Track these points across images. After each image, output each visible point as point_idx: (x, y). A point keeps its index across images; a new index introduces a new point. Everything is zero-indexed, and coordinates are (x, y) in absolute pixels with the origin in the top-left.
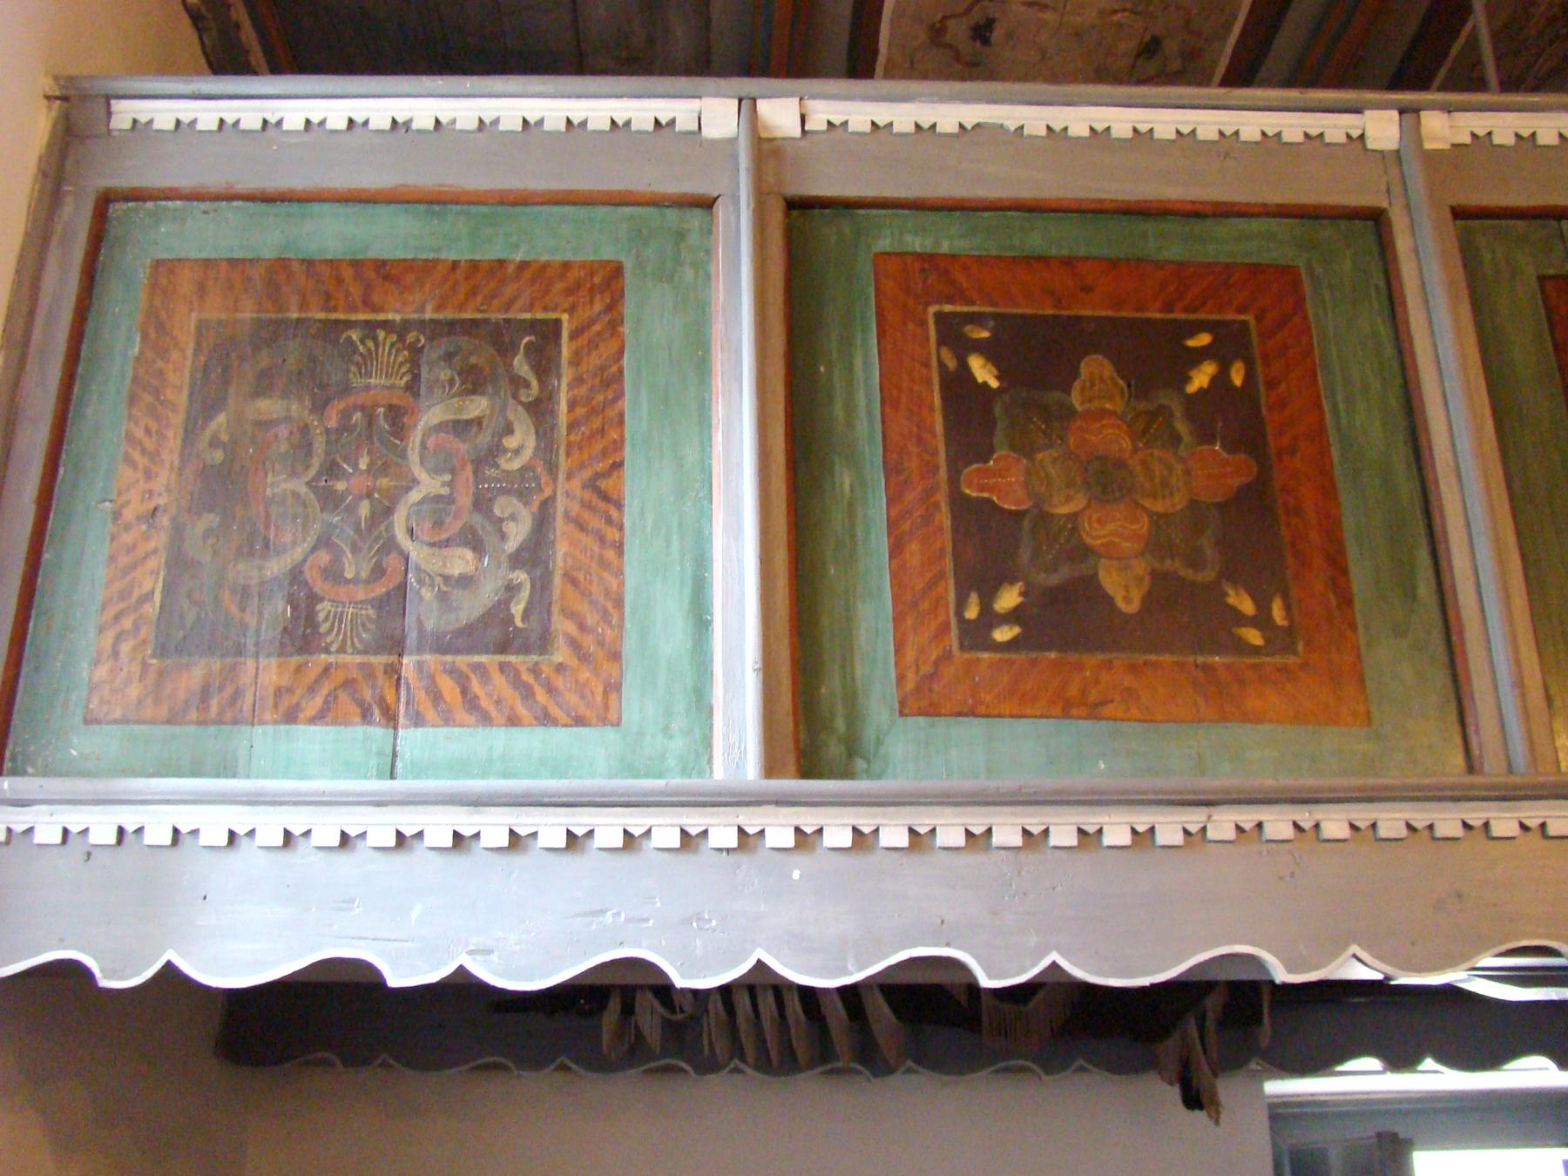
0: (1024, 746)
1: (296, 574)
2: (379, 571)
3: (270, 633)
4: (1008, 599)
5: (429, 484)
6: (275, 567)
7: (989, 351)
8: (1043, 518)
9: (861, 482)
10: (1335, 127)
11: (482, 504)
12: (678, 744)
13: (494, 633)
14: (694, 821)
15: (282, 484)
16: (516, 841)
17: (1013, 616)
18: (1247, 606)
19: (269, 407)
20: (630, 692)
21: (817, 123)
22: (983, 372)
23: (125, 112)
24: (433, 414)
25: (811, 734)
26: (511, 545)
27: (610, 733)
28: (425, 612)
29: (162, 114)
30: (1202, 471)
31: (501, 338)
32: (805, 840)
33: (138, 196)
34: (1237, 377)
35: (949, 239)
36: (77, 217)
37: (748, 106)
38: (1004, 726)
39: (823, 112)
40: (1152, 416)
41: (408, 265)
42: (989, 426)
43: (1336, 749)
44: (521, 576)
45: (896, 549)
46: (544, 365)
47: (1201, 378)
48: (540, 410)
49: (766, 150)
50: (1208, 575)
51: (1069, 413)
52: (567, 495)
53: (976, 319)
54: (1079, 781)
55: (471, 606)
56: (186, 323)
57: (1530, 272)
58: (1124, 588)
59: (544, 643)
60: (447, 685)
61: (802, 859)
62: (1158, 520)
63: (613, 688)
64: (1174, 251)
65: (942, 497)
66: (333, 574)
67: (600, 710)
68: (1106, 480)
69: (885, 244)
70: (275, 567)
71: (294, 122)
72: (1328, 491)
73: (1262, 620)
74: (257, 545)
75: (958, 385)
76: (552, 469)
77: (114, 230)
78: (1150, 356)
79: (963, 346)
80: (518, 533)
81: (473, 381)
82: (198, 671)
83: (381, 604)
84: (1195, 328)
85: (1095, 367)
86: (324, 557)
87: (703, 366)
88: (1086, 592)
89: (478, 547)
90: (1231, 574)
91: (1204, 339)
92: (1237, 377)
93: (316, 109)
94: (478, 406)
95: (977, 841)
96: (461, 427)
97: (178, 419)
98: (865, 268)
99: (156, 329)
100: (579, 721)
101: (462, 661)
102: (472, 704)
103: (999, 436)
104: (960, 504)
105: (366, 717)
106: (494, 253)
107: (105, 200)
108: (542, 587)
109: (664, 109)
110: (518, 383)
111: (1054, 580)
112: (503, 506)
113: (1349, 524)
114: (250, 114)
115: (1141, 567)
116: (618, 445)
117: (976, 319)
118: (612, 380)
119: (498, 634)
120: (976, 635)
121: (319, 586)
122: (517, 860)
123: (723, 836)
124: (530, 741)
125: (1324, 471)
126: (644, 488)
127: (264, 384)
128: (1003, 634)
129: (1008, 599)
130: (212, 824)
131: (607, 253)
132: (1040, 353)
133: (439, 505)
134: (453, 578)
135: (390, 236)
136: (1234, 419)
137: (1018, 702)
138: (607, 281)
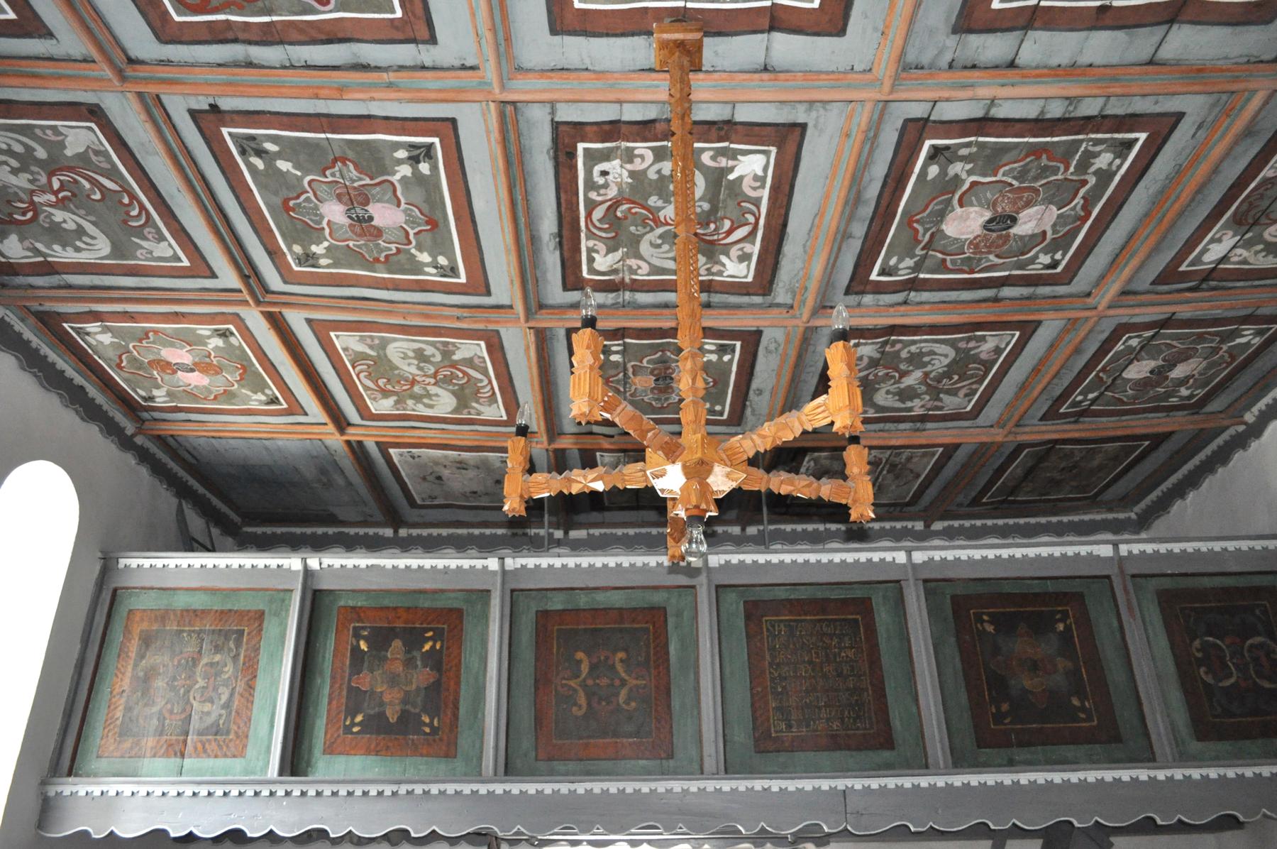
0: (357, 764)
1: (160, 712)
2: (184, 710)
3: (152, 729)
4: (359, 718)
5: (201, 683)
6: (155, 709)
7: (366, 639)
8: (373, 693)
9: (323, 682)
10: (479, 563)
11: (215, 689)
12: (261, 763)
13: (214, 730)
14: (258, 788)
16: (210, 794)
17: (359, 724)
18: (427, 720)
20: (249, 748)
21: (325, 565)
23: (123, 562)
24: (205, 661)
25: (295, 761)
26: (222, 702)
27: (242, 760)
28: (195, 724)
29: (134, 563)
32: (288, 794)
33: (127, 588)
34: (438, 647)
36: (106, 596)
37: (304, 560)
38: (351, 758)
39: (327, 561)
40: (410, 659)
41: (203, 611)
42: (363, 661)
43: (441, 766)
44: (223, 712)
45: (330, 703)
46: (238, 645)
47: (427, 647)
49: (308, 573)
50: (417, 711)
51: (386, 658)
53: (363, 628)
54: (369, 776)
55: (210, 720)
57: (534, 609)
58: (392, 715)
59: (228, 733)
60: (199, 745)
61: (287, 799)
62: (407, 693)
63: (245, 746)
64: (427, 604)
65: (345, 687)
66: (171, 712)
67: (240, 754)
68: (393, 681)
69: (342, 603)
70: (155, 709)
71: (172, 566)
72: (458, 684)
73: (431, 725)
75: (356, 650)
76: (236, 678)
77: (118, 599)
78: (413, 638)
79: (357, 636)
80: (224, 698)
81: (218, 649)
83: (183, 721)
85: (397, 644)
86: (169, 706)
87: (283, 643)
88: (382, 715)
89: (212, 702)
90: (425, 710)
91: (430, 634)
92: (438, 647)
93: (178, 561)
94: (218, 658)
95: (334, 794)
96: (211, 664)
97: (132, 662)
98: (335, 612)
100: (234, 756)
101: (204, 738)
102: (205, 750)
103: (366, 665)
104: (350, 689)
105: (175, 755)
106: (229, 607)
107: (115, 590)
109: (280, 561)
110: (230, 650)
111: (372, 712)
113: (462, 693)
114: (159, 563)
115: (398, 708)
116: (256, 670)
117: (363, 628)
118: (257, 650)
120: (348, 729)
121: (167, 715)
122: (210, 799)
123: (266, 793)
124: (220, 763)
125: (458, 677)
126: (261, 684)
128: (355, 729)
129: (359, 718)
130: (127, 790)
131: (261, 607)
132: (381, 639)
136: (435, 660)
138: (261, 615)
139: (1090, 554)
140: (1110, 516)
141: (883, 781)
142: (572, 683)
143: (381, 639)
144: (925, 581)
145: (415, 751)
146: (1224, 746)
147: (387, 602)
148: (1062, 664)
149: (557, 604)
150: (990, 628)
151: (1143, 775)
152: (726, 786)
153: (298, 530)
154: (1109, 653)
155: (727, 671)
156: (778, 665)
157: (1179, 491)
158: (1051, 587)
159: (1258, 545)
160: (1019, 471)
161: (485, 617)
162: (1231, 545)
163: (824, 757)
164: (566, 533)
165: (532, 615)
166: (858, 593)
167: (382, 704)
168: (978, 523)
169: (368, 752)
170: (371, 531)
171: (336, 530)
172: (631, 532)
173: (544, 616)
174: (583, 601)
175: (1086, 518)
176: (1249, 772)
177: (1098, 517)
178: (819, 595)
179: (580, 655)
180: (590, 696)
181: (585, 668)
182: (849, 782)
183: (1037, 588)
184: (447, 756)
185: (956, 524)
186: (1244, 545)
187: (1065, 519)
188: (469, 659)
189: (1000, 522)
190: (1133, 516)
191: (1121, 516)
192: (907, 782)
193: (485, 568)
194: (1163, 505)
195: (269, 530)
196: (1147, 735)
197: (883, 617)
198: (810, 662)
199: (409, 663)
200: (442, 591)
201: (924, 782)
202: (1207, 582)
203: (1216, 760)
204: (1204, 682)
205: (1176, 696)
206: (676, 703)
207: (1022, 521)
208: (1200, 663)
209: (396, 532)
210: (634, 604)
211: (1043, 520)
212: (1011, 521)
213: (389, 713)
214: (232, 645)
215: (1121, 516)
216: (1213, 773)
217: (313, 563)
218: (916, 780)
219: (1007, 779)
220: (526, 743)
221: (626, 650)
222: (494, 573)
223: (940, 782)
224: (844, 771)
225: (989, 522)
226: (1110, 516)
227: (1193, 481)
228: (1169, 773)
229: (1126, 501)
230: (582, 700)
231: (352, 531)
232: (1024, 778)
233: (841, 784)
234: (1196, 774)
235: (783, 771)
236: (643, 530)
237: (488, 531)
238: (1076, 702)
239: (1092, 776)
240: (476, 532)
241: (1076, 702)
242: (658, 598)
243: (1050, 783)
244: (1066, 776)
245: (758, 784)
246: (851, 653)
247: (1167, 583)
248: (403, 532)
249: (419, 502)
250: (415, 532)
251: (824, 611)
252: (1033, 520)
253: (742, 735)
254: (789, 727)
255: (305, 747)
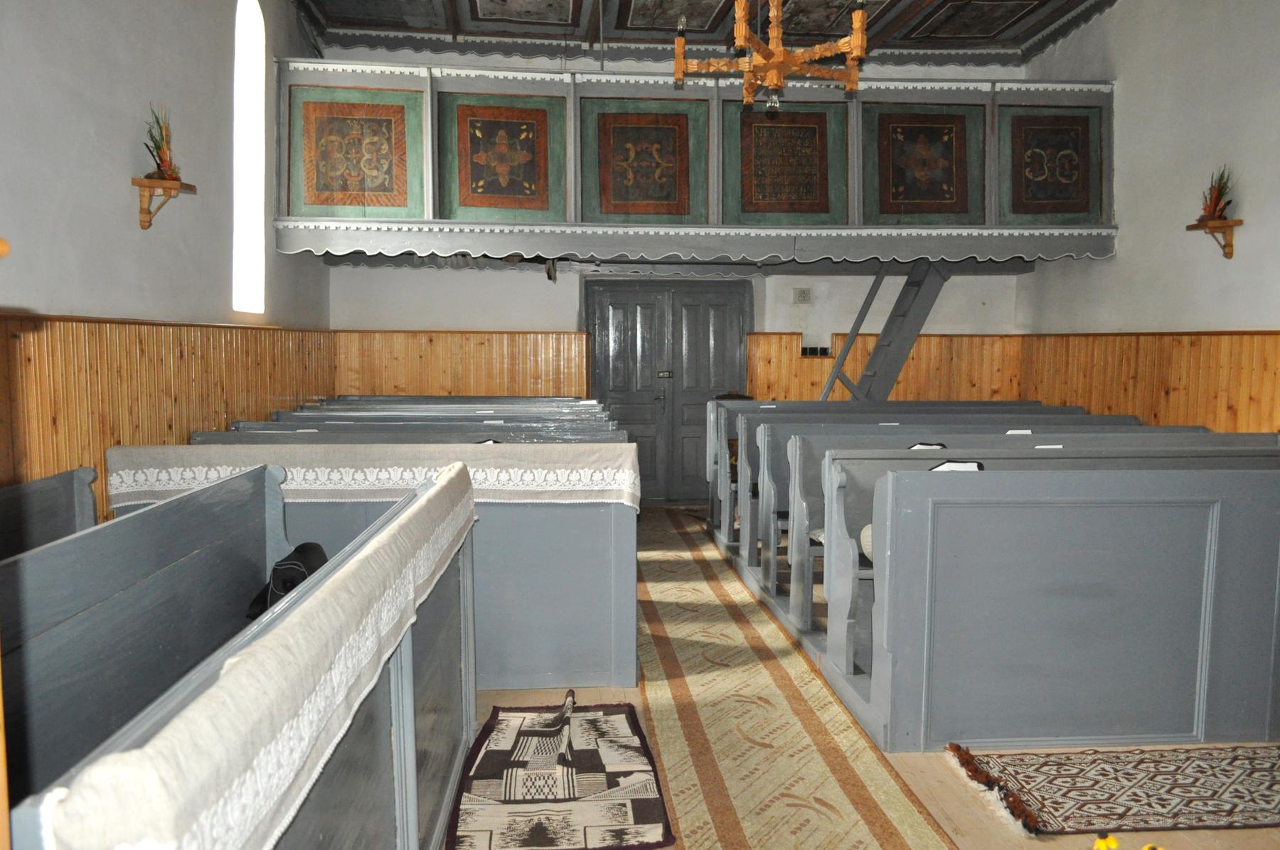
0: (483, 212)
4: (481, 183)
5: (367, 156)
7: (481, 130)
8: (489, 167)
11: (378, 160)
15: (338, 155)
19: (333, 138)
22: (478, 134)
24: (367, 140)
25: (442, 210)
28: (368, 183)
30: (521, 157)
31: (379, 122)
32: (441, 230)
35: (473, 102)
36: (285, 91)
37: (430, 69)
43: (539, 214)
46: (389, 130)
47: (523, 136)
48: (389, 139)
52: (395, 159)
54: (490, 220)
55: (378, 182)
56: (313, 117)
57: (596, 112)
58: (504, 182)
66: (350, 175)
67: (403, 203)
68: (502, 158)
69: (460, 102)
70: (338, 173)
73: (530, 189)
74: (334, 168)
75: (473, 136)
78: (513, 133)
79: (475, 128)
80: (386, 167)
81: (375, 133)
82: (327, 194)
84: (522, 124)
85: (502, 133)
90: (524, 179)
94: (376, 139)
95: (472, 231)
96: (373, 144)
99: (307, 119)
106: (376, 102)
107: (290, 86)
108: (391, 178)
112: (383, 161)
119: (383, 188)
126: (410, 158)
127: (331, 134)
129: (481, 183)
130: (333, 225)
131: (401, 103)
132: (491, 129)
133: (369, 161)
134: (374, 176)
135: (355, 98)
137: (482, 205)
138: (401, 110)
139: (976, 89)
140: (1002, 51)
141: (819, 232)
142: (624, 164)
143: (491, 129)
144: (864, 103)
145: (521, 205)
146: (1029, 217)
147: (491, 103)
148: (942, 163)
149: (612, 109)
150: (901, 137)
151: (975, 232)
152: (723, 232)
153: (374, 33)
154: (973, 158)
155: (727, 160)
156: (761, 157)
157: (1053, 38)
158: (945, 110)
159: (1085, 87)
160: (942, 17)
161: (562, 117)
162: (1068, 87)
163: (783, 216)
164: (591, 46)
165: (595, 116)
166: (818, 110)
167: (496, 174)
168: (905, 52)
169: (490, 205)
170: (434, 36)
171: (406, 34)
172: (642, 46)
173: (603, 117)
174: (631, 107)
175: (985, 52)
176: (1037, 233)
177: (993, 52)
178: (792, 110)
179: (629, 145)
180: (635, 173)
181: (632, 154)
182: (798, 232)
183: (937, 111)
184: (542, 209)
185: (889, 51)
186: (1077, 87)
187: (969, 52)
188: (553, 147)
189: (921, 52)
190: (1019, 52)
191: (1010, 51)
192: (834, 233)
193: (562, 81)
194: (1041, 46)
195: (349, 32)
196: (984, 209)
197: (832, 127)
198: (782, 156)
199: (511, 147)
200: (531, 96)
201: (844, 233)
202: (1045, 112)
203: (1021, 225)
204: (1027, 178)
205: (1007, 185)
206: (692, 180)
207: (937, 52)
208: (1027, 165)
209: (455, 38)
210: (665, 111)
211: (953, 52)
212: (929, 52)
213: (501, 179)
214: (384, 130)
215: (1010, 51)
216: (1016, 233)
217: (437, 72)
218: (840, 232)
219: (895, 232)
220: (595, 202)
221: (660, 143)
222: (568, 84)
223: (854, 233)
224: (795, 225)
225: (913, 52)
226: (1002, 51)
227: (1063, 32)
228: (990, 231)
229: (1016, 41)
230: (631, 176)
231: (419, 36)
232: (905, 232)
233: (793, 232)
234: (1006, 232)
235: (758, 224)
236: (652, 46)
237: (529, 41)
238: (945, 187)
239: (945, 232)
240: (520, 41)
241: (945, 187)
242: (682, 108)
243: (919, 236)
244: (929, 231)
245: (743, 232)
246: (808, 151)
247: (1021, 112)
248: (460, 38)
249: (480, 16)
250: (470, 39)
251: (794, 122)
252: (945, 52)
253: (734, 203)
254: (764, 197)
255: (446, 200)
